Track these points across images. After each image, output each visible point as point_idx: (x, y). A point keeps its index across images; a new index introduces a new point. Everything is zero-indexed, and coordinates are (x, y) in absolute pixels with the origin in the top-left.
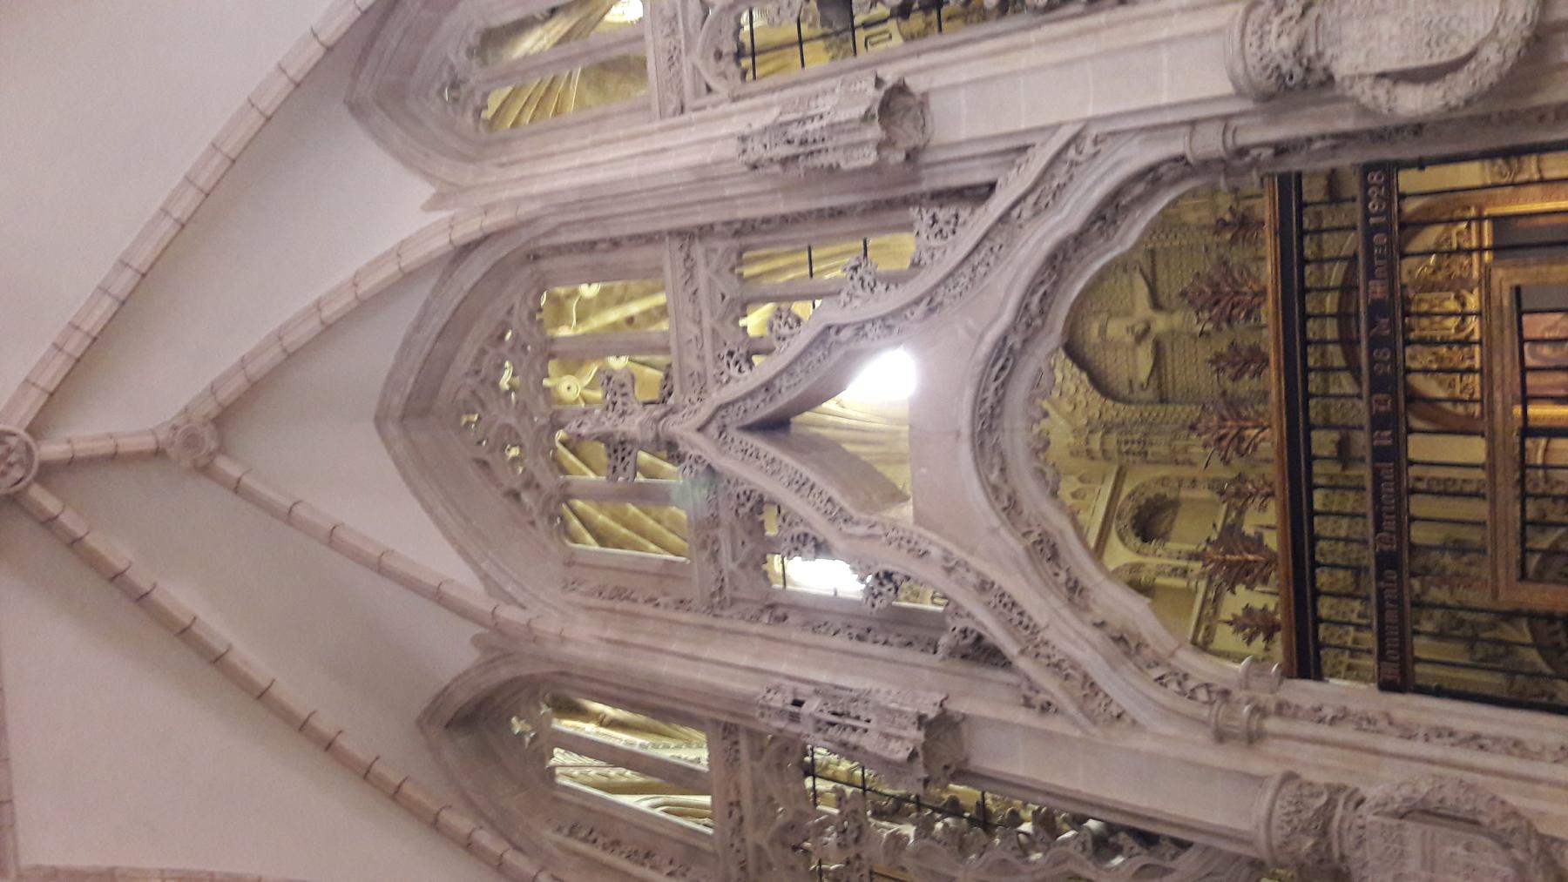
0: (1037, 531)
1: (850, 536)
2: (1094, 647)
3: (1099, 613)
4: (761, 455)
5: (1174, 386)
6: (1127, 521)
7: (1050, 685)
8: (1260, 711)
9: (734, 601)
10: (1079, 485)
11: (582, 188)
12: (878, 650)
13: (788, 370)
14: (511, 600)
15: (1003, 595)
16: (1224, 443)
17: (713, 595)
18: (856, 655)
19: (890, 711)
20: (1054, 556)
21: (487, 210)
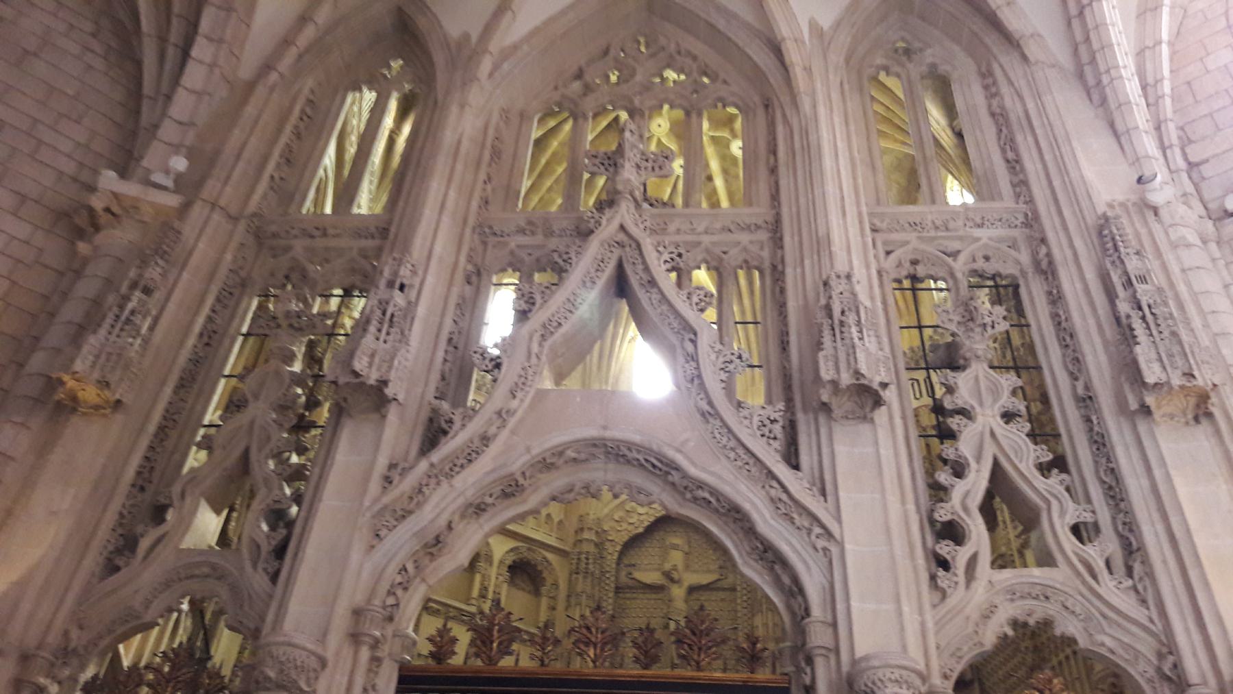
0: (526, 483)
1: (531, 338)
2: (432, 521)
3: (459, 527)
4: (599, 274)
5: (629, 599)
6: (526, 554)
7: (406, 485)
8: (376, 644)
9: (485, 243)
10: (556, 520)
11: (819, 147)
12: (440, 354)
13: (664, 298)
14: (496, 67)
15: (478, 453)
16: (584, 631)
17: (491, 227)
18: (437, 336)
19: (392, 359)
20: (506, 495)
21: (808, 70)
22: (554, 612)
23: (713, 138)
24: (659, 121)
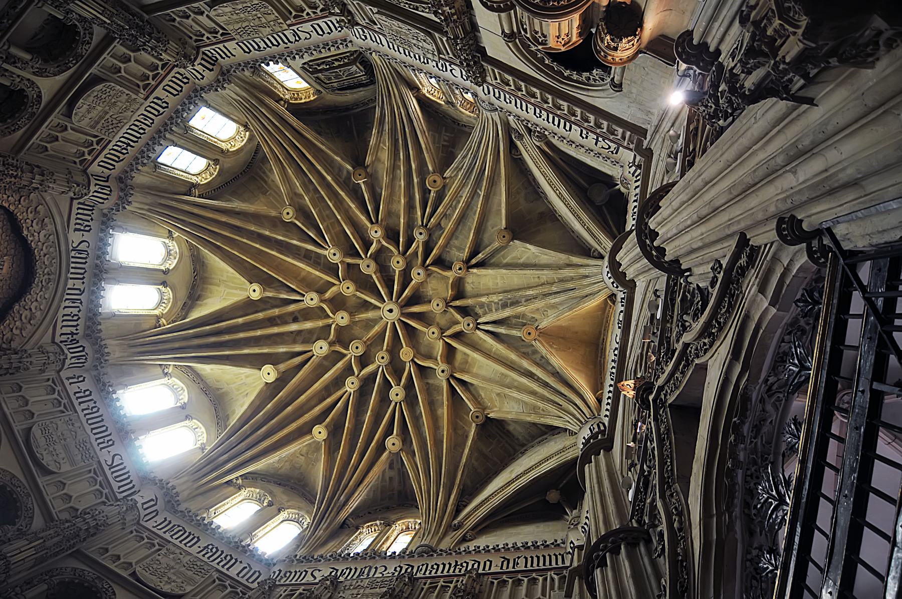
10: (48, 145)
23: (330, 326)
24: (352, 288)
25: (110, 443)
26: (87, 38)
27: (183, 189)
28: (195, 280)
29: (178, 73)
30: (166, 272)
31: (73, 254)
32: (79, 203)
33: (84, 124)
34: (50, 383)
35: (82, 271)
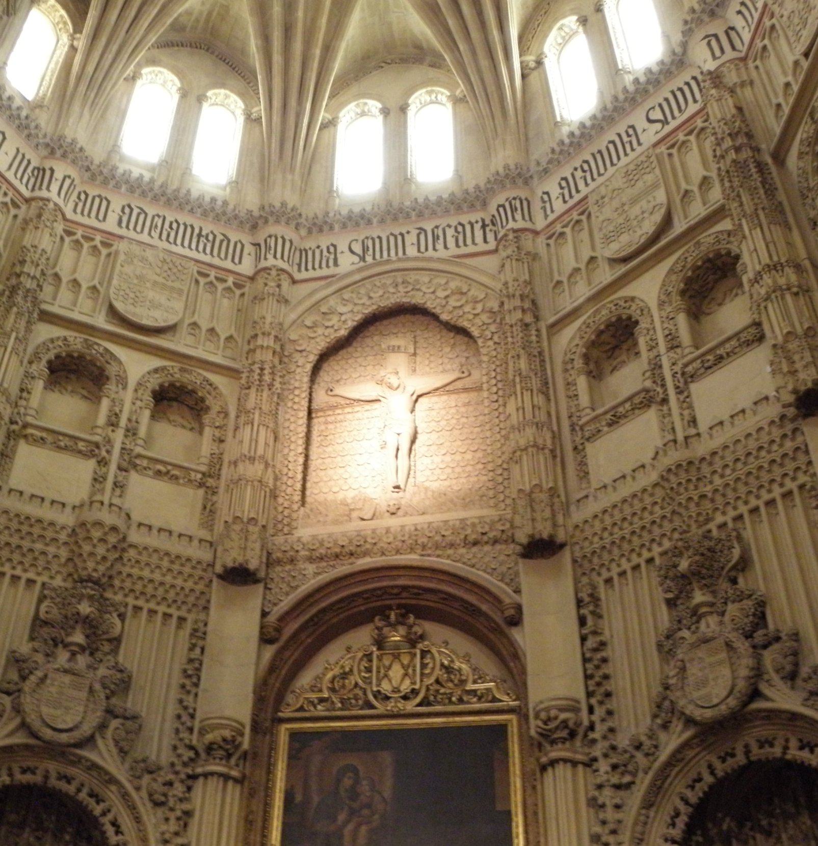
6: (178, 376)
22: (222, 445)
25: (631, 132)
26: (60, 343)
27: (257, 130)
28: (393, 62)
29: (75, 211)
30: (385, 112)
31: (369, 259)
32: (299, 270)
33: (179, 305)
34: (551, 242)
35: (392, 239)
